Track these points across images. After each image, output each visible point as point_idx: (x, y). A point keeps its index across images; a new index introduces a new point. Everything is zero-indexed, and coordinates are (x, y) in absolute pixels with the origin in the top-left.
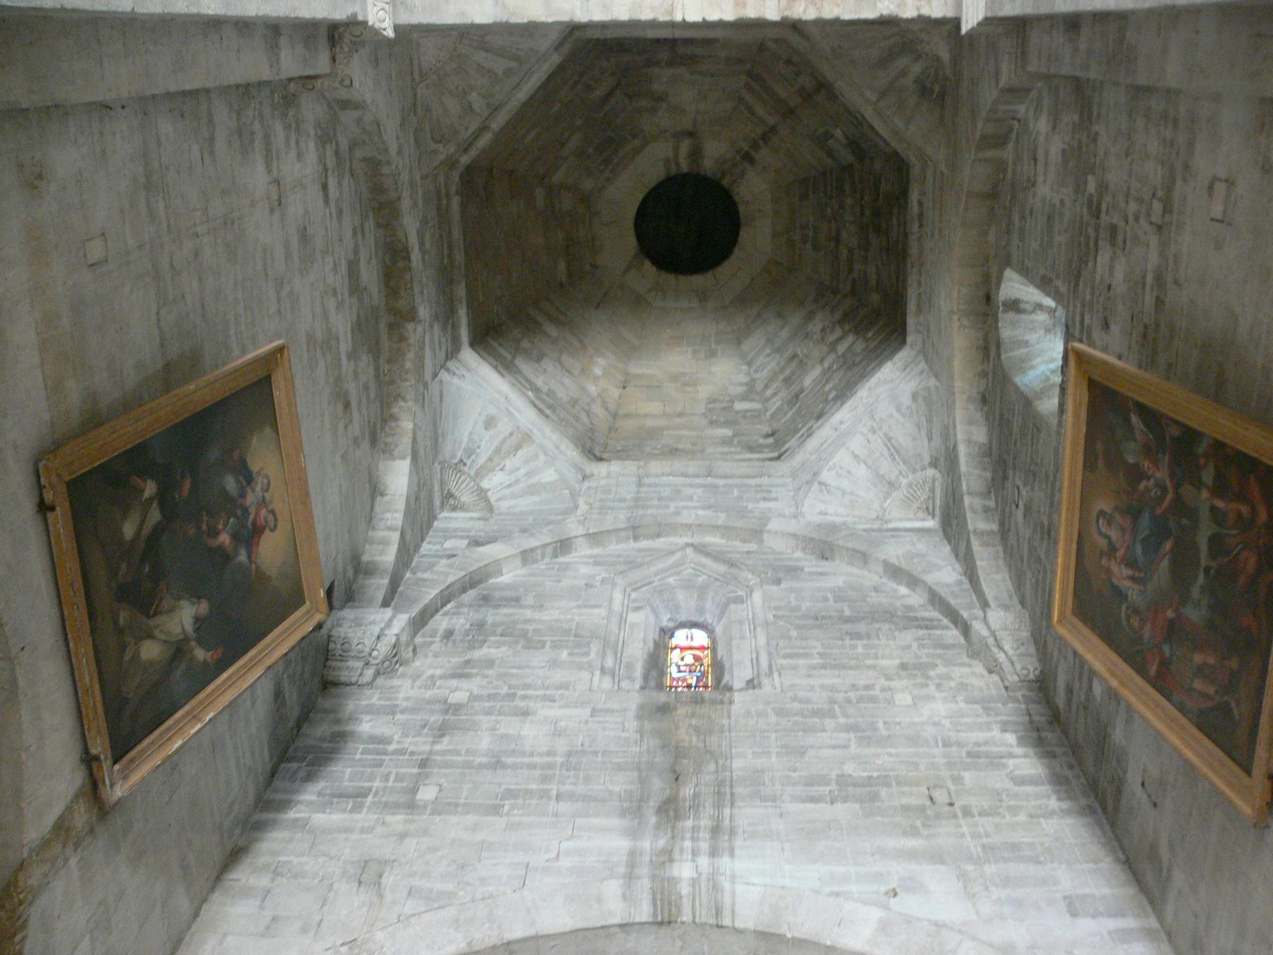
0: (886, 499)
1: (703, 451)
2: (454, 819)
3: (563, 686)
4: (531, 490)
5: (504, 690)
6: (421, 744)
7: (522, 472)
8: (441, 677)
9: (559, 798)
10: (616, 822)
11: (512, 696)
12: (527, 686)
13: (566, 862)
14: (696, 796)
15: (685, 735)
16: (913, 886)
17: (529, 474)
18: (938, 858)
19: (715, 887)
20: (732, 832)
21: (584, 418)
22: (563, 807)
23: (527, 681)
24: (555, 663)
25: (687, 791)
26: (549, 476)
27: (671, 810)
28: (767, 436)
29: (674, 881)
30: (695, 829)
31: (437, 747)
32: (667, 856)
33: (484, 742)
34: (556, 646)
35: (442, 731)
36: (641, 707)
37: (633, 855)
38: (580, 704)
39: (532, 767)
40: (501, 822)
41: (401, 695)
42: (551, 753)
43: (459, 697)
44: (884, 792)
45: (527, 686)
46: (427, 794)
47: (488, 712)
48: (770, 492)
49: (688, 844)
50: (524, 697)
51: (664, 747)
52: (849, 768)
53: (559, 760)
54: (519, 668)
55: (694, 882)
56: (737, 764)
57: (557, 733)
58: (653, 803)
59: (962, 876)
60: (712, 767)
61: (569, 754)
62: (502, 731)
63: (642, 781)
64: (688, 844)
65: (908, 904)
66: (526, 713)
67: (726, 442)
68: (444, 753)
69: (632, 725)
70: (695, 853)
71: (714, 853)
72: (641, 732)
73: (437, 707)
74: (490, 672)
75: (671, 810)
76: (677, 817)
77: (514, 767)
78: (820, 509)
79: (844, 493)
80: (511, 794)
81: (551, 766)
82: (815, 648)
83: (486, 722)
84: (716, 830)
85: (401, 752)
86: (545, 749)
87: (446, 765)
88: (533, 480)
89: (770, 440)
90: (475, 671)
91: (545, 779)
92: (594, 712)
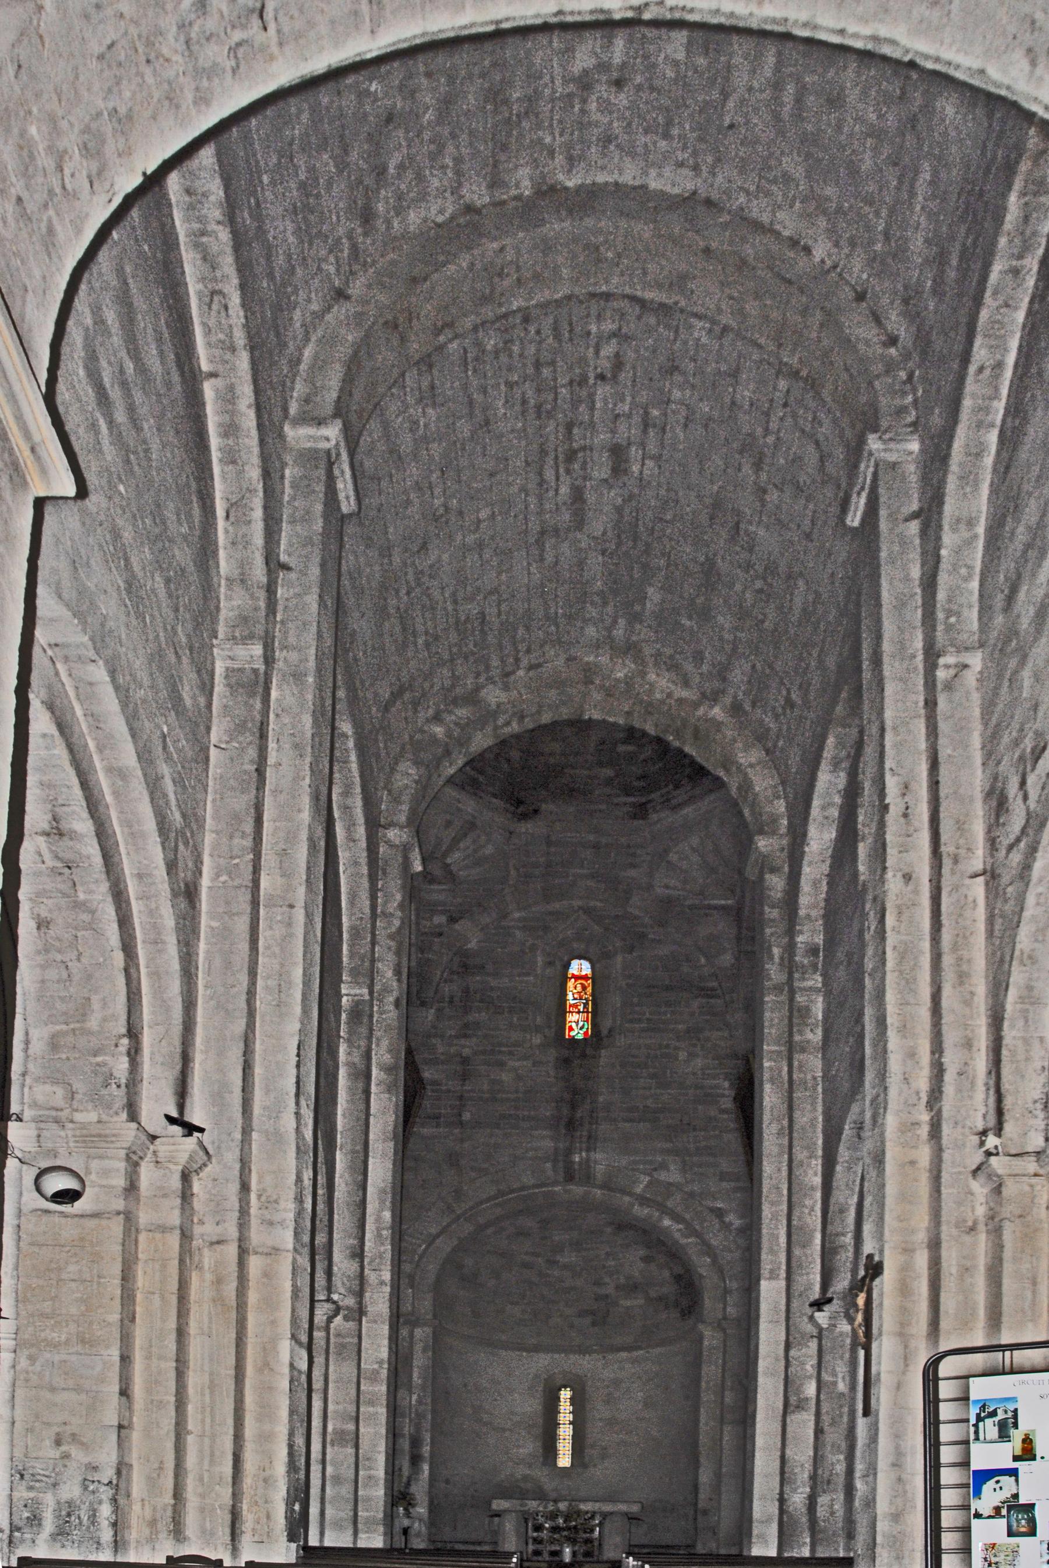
3: (517, 1044)
5: (489, 1048)
8: (457, 1037)
12: (500, 1045)
13: (530, 1154)
16: (663, 1166)
18: (675, 1152)
19: (589, 1167)
25: (579, 1115)
26: (489, 850)
27: (571, 1125)
28: (639, 779)
29: (573, 1163)
30: (581, 1137)
32: (569, 1152)
34: (511, 1011)
35: (464, 1077)
43: (466, 1052)
44: (661, 1116)
45: (500, 1045)
46: (467, 1116)
48: (634, 855)
52: (649, 1102)
55: (580, 1163)
56: (601, 1099)
57: (519, 1078)
59: (684, 1162)
65: (663, 1176)
66: (501, 1064)
67: (609, 782)
68: (469, 1091)
69: (552, 1073)
71: (588, 1150)
75: (571, 1125)
78: (665, 884)
84: (589, 1137)
89: (642, 784)
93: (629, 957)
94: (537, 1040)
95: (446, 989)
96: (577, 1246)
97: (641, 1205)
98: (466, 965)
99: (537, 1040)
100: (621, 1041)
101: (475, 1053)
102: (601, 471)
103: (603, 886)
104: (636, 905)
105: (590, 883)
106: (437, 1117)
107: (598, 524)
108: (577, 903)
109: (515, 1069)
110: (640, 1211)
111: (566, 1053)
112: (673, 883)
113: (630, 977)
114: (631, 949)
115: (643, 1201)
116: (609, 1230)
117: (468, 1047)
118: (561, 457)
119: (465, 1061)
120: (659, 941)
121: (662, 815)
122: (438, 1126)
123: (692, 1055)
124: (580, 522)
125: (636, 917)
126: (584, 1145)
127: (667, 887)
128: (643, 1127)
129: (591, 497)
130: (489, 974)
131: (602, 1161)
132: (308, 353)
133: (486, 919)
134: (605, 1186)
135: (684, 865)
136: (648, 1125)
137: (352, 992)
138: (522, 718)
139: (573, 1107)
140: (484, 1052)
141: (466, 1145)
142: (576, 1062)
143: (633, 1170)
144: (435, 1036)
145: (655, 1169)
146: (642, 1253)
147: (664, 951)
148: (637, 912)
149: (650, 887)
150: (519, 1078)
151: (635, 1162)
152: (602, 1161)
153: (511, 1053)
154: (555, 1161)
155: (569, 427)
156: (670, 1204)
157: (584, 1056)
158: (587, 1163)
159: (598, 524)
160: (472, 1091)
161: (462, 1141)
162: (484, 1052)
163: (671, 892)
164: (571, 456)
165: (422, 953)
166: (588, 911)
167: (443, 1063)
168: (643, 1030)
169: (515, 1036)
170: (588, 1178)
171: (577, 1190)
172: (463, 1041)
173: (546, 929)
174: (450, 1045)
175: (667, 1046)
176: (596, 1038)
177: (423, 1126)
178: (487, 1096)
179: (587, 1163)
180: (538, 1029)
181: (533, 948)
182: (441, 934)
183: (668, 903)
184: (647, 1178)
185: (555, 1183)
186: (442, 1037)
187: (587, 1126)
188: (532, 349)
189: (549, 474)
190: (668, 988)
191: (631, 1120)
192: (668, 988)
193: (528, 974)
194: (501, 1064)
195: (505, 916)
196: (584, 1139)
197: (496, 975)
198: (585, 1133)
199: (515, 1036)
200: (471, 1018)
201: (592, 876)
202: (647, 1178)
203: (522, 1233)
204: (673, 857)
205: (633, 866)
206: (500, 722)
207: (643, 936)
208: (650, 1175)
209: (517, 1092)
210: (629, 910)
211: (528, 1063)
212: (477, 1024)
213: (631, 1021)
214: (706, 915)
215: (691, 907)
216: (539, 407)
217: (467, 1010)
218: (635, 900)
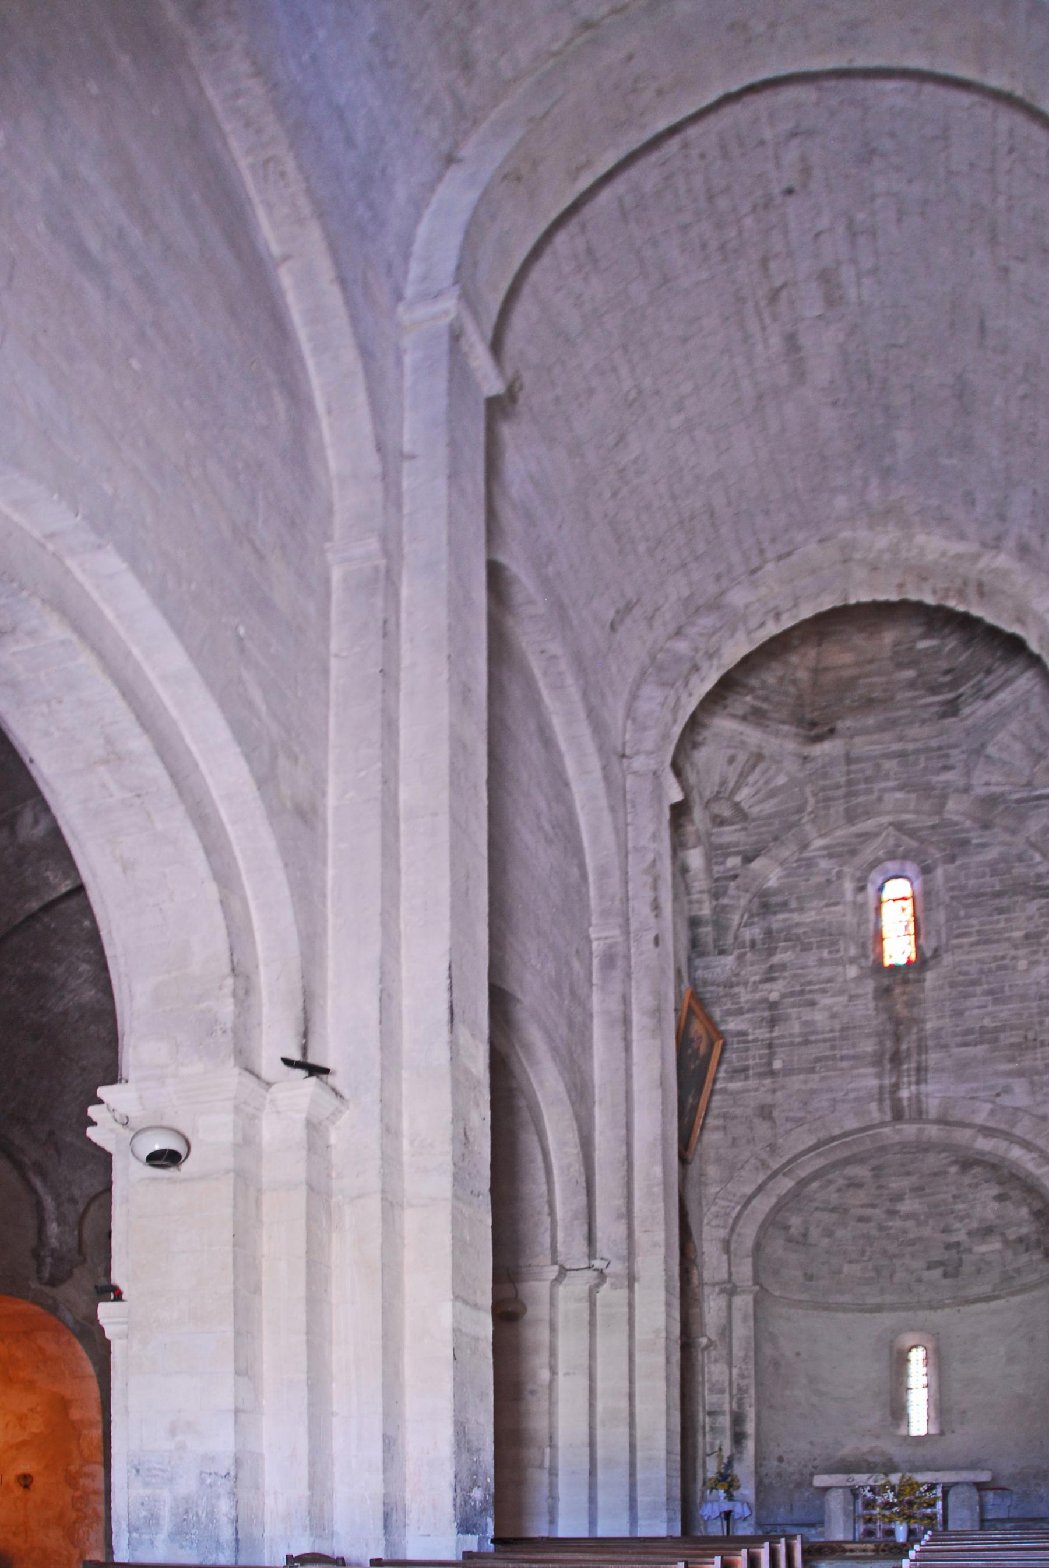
0: (1035, 765)
1: (892, 698)
2: (795, 1078)
3: (830, 980)
4: (772, 794)
5: (798, 988)
6: (762, 1033)
7: (761, 782)
9: (842, 1058)
10: (871, 1070)
11: (802, 992)
12: (810, 983)
14: (908, 1049)
15: (901, 1010)
16: (1007, 1090)
17: (767, 782)
18: (1021, 1073)
20: (926, 1070)
21: (792, 690)
22: (845, 1064)
23: (809, 978)
24: (822, 962)
25: (904, 1047)
30: (909, 1069)
31: (775, 1034)
33: (796, 1028)
35: (773, 1023)
36: (876, 991)
37: (881, 1087)
38: (841, 992)
39: (825, 1041)
40: (816, 1077)
41: (743, 999)
42: (832, 1031)
43: (774, 996)
44: (1002, 1036)
45: (810, 983)
46: (777, 1064)
47: (793, 1006)
48: (947, 756)
49: (905, 1079)
50: (811, 992)
51: (890, 1018)
52: (987, 1022)
53: (838, 1034)
54: (801, 968)
55: (910, 1099)
56: (929, 1026)
57: (833, 1016)
58: (888, 1056)
59: (1032, 1083)
60: (915, 1030)
61: (842, 1030)
62: (804, 1019)
63: (881, 1043)
64: (905, 1079)
65: (1006, 1100)
66: (812, 1004)
68: (778, 1038)
69: (872, 1005)
70: (910, 1084)
71: (918, 1083)
72: (876, 1009)
73: (764, 1005)
74: (786, 974)
75: (896, 1059)
76: (900, 1064)
77: (817, 1041)
78: (987, 780)
79: (1005, 763)
80: (818, 1060)
81: (833, 1039)
82: (972, 926)
83: (793, 1012)
84: (919, 1069)
85: (755, 1040)
86: (828, 1028)
87: (782, 1045)
88: (771, 786)
90: (777, 974)
91: (833, 1048)
92: (851, 998)
93: (951, 867)
94: (852, 972)
95: (747, 934)
96: (918, 1190)
97: (985, 1136)
98: (766, 905)
99: (852, 972)
100: (947, 959)
101: (784, 996)
102: (812, 307)
103: (913, 796)
104: (955, 808)
105: (899, 795)
106: (746, 1069)
107: (821, 373)
108: (886, 819)
109: (829, 1008)
110: (983, 1144)
111: (886, 982)
112: (995, 778)
113: (952, 889)
114: (952, 859)
115: (987, 1131)
116: (953, 1169)
117: (774, 991)
118: (763, 303)
119: (773, 1006)
120: (984, 845)
121: (976, 706)
122: (747, 1078)
123: (1033, 964)
124: (800, 375)
125: (956, 824)
126: (913, 1079)
127: (987, 784)
128: (981, 1050)
129: (806, 341)
130: (792, 911)
131: (935, 1093)
132: (422, 231)
133: (785, 853)
134: (942, 1121)
135: (1005, 756)
136: (985, 1047)
137: (604, 934)
138: (777, 616)
139: (898, 1039)
140: (792, 994)
141: (779, 1094)
142: (898, 990)
143: (972, 1098)
144: (738, 984)
145: (998, 1095)
146: (995, 1191)
147: (992, 854)
148: (956, 818)
149: (967, 790)
150: (833, 1016)
151: (977, 1090)
152: (935, 1093)
153: (823, 991)
154: (881, 1100)
155: (764, 262)
156: (1018, 1131)
157: (906, 982)
158: (917, 1098)
159: (821, 373)
160: (783, 1037)
161: (774, 1091)
162: (792, 994)
163: (994, 789)
164: (774, 297)
165: (717, 899)
166: (899, 826)
167: (748, 1011)
168: (972, 945)
169: (827, 972)
170: (920, 1115)
171: (909, 1130)
172: (768, 986)
173: (853, 853)
174: (754, 991)
175: (1003, 958)
176: (920, 963)
177: (731, 1079)
178: (798, 1040)
179: (917, 1098)
180: (852, 961)
181: (840, 875)
182: (735, 877)
183: (990, 801)
184: (988, 1106)
185: (882, 1124)
186: (746, 984)
187: (914, 1057)
188: (698, 180)
189: (753, 326)
190: (997, 895)
191: (966, 1044)
192: (997, 895)
193: (837, 904)
194: (812, 1004)
195: (804, 846)
196: (913, 1073)
197: (801, 910)
198: (913, 1065)
199: (827, 972)
200: (777, 959)
201: (900, 788)
202: (988, 1106)
203: (855, 1184)
204: (991, 750)
205: (947, 768)
206: (753, 623)
207: (966, 842)
208: (993, 1102)
209: (832, 1031)
210: (947, 816)
211: (844, 999)
212: (783, 967)
213: (958, 936)
214: (1037, 807)
215: (1019, 801)
216: (722, 247)
217: (771, 952)
218: (951, 805)
